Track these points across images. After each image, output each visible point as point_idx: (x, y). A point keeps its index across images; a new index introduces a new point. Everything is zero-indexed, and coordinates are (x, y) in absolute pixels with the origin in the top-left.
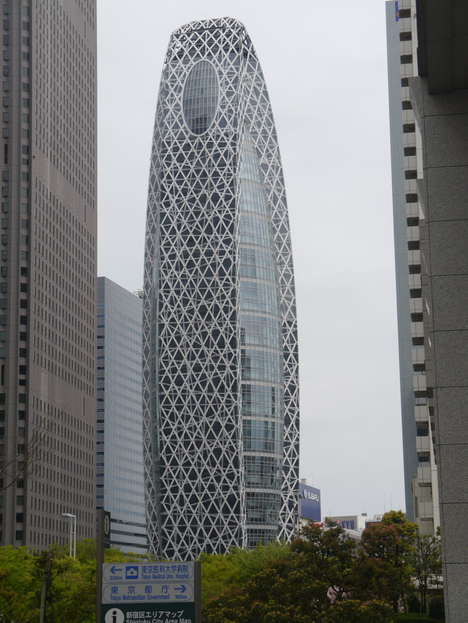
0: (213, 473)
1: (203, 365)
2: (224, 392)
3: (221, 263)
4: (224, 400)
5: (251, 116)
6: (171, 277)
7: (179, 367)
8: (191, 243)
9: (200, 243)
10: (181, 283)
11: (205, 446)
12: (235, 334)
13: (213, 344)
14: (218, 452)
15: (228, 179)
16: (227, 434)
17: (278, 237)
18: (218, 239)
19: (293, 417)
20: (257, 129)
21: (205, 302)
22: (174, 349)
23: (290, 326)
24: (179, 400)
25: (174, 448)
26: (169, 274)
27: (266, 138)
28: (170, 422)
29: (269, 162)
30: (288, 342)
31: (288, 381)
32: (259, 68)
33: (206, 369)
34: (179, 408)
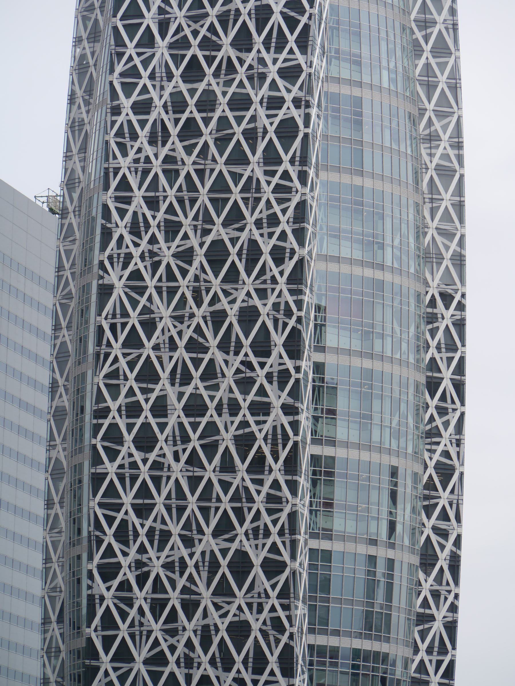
1: (212, 398)
2: (262, 472)
3: (271, 130)
4: (263, 494)
6: (136, 161)
7: (147, 400)
8: (193, 72)
9: (216, 74)
10: (163, 180)
11: (205, 615)
12: (299, 320)
13: (239, 346)
14: (239, 631)
16: (267, 585)
17: (428, 65)
18: (265, 65)
19: (442, 547)
21: (222, 231)
22: (135, 352)
23: (447, 307)
24: (144, 488)
25: (124, 615)
26: (132, 154)
28: (116, 546)
30: (438, 348)
31: (434, 451)
33: (219, 409)
34: (142, 511)
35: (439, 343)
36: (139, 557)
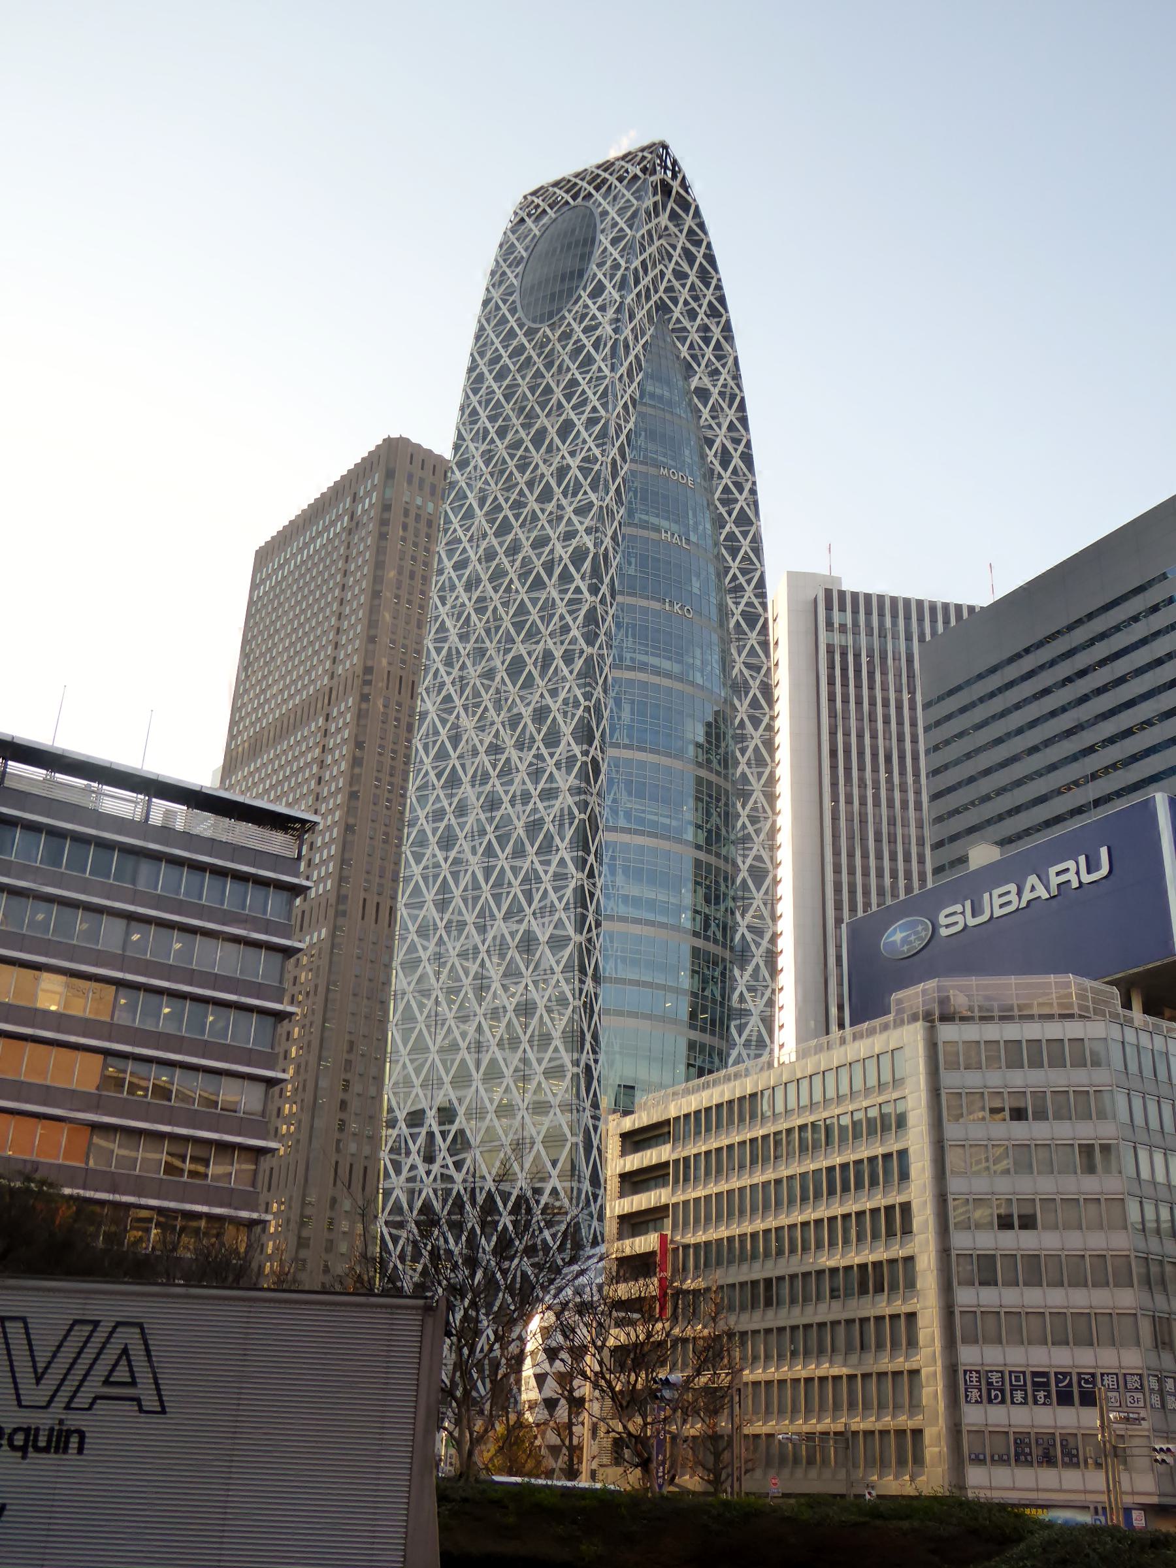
0: (512, 1069)
1: (506, 792)
3: (566, 557)
4: (550, 874)
5: (675, 301)
6: (453, 607)
8: (504, 528)
15: (595, 386)
18: (563, 509)
19: (758, 945)
20: (686, 323)
23: (756, 729)
26: (450, 602)
27: (707, 340)
30: (748, 764)
32: (697, 213)
33: (512, 802)
35: (749, 759)
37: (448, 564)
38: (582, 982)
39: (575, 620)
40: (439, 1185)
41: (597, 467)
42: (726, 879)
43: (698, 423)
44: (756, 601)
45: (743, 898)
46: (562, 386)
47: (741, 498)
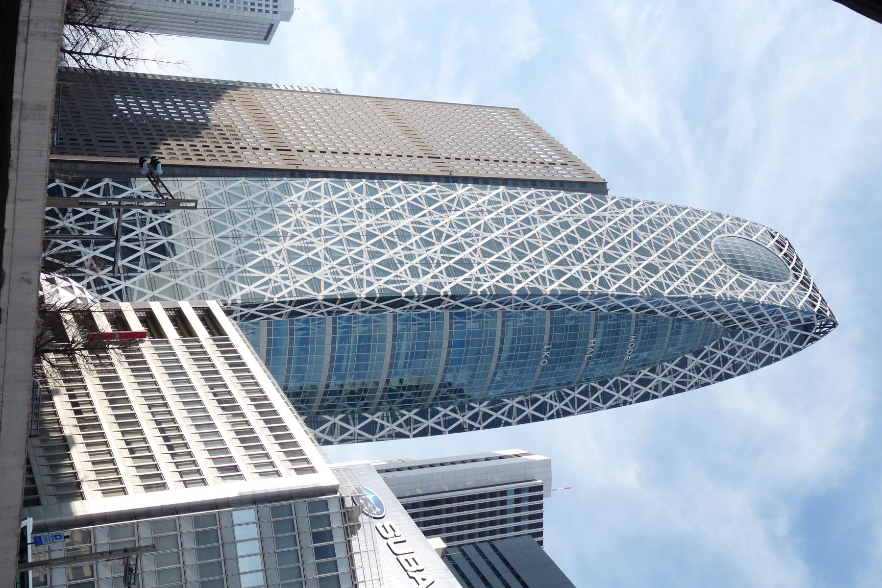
0: (224, 260)
8: (584, 234)
16: (302, 282)
20: (727, 348)
22: (423, 202)
23: (470, 418)
27: (717, 363)
29: (690, 371)
30: (445, 415)
31: (383, 419)
32: (796, 350)
36: (299, 206)
37: (554, 198)
38: (290, 303)
39: (532, 281)
40: (137, 218)
41: (632, 289)
42: (366, 405)
43: (665, 361)
44: (554, 411)
45: (354, 419)
46: (679, 265)
47: (620, 395)
